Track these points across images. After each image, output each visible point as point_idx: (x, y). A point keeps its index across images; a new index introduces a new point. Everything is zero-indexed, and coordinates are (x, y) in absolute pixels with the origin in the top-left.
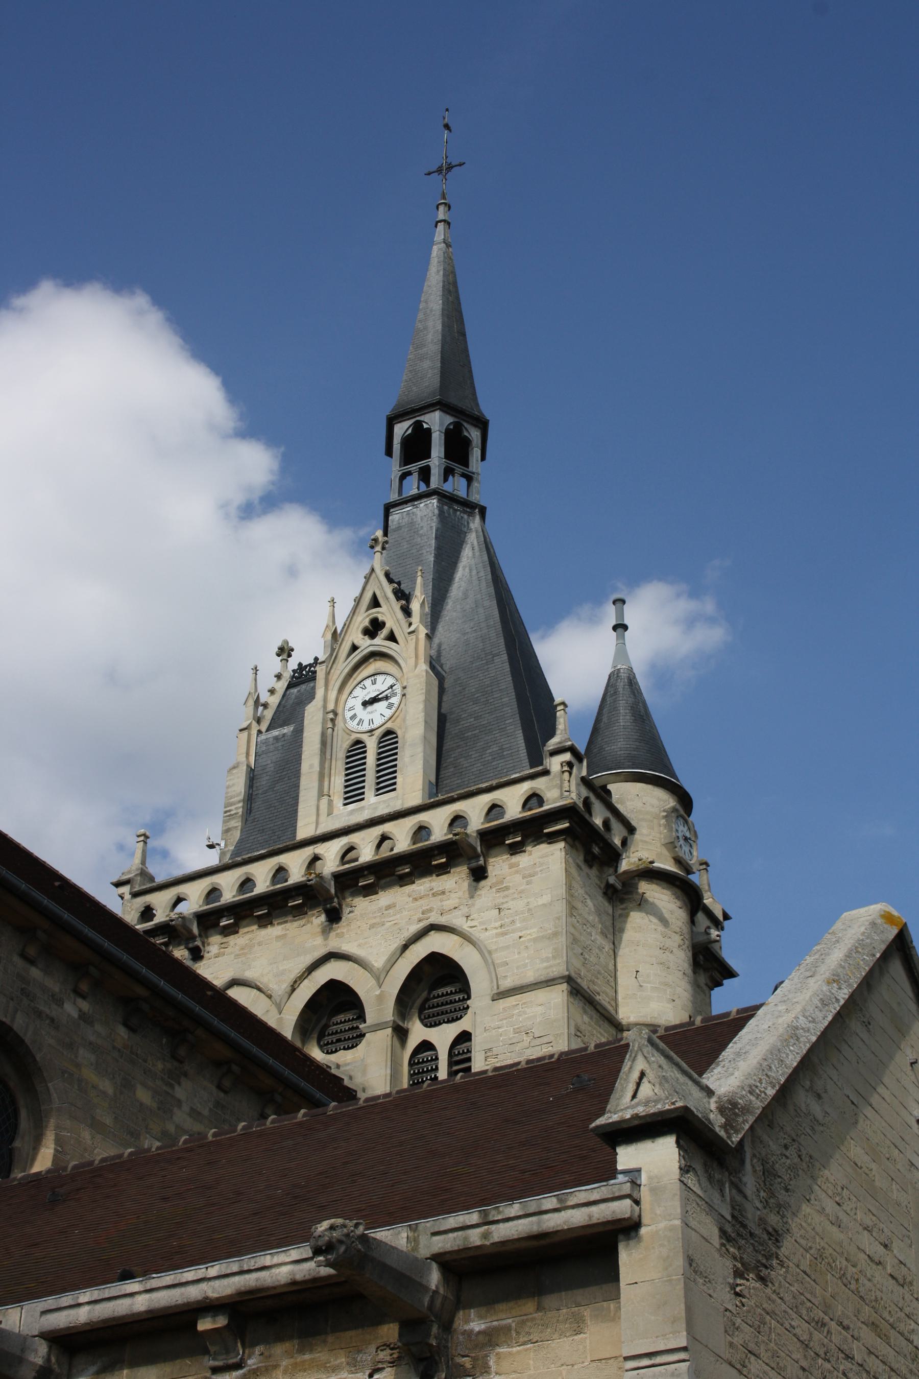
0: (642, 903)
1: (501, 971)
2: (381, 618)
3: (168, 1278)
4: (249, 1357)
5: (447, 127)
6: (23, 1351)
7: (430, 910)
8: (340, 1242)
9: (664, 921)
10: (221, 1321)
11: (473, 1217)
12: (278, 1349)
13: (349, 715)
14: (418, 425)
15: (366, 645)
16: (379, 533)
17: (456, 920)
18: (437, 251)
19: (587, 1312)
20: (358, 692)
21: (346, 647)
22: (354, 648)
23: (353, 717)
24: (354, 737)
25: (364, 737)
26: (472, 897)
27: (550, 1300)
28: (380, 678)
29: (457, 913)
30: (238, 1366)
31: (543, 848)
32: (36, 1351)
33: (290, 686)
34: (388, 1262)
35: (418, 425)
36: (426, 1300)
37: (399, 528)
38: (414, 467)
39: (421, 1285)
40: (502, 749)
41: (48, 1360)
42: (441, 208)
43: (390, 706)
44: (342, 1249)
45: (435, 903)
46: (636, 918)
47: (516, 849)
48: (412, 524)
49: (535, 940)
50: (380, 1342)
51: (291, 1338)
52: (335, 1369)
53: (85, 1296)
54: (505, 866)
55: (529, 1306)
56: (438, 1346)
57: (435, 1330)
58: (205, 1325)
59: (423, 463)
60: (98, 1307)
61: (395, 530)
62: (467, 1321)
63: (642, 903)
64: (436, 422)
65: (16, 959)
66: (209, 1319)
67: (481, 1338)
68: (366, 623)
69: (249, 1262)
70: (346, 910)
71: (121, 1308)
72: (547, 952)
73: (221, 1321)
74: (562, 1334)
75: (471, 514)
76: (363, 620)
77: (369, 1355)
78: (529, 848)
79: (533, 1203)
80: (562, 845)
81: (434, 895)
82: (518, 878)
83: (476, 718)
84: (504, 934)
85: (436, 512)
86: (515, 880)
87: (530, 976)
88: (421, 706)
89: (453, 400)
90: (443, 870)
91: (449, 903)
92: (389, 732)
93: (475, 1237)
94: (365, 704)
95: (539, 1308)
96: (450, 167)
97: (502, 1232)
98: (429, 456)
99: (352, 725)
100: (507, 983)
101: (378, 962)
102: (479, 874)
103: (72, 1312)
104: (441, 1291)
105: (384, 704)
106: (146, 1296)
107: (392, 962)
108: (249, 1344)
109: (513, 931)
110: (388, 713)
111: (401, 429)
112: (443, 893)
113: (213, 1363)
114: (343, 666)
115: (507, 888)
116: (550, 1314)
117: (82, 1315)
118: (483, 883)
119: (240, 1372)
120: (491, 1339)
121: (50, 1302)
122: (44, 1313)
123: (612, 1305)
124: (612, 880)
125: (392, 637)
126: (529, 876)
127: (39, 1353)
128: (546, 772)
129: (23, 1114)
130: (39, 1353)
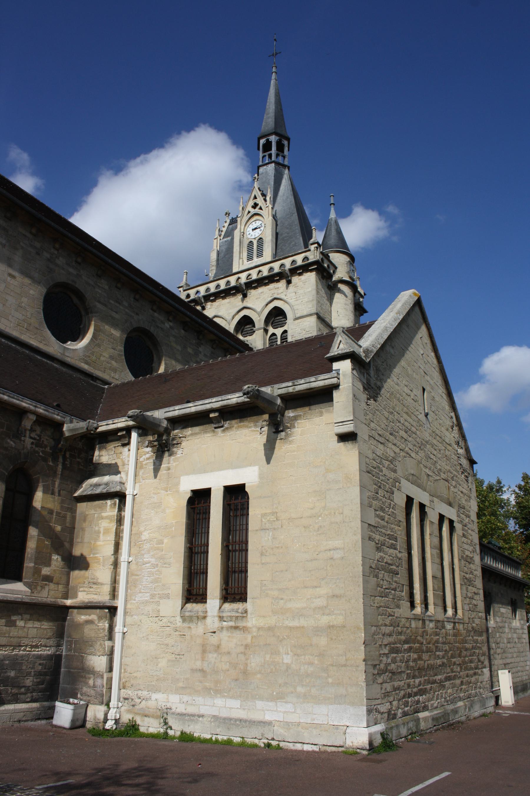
0: (339, 291)
1: (296, 312)
2: (257, 202)
3: (201, 402)
4: (225, 424)
5: (275, 40)
6: (160, 423)
7: (274, 293)
8: (251, 391)
9: (346, 296)
10: (217, 414)
11: (290, 384)
12: (234, 422)
14: (268, 140)
15: (253, 211)
16: (256, 175)
17: (282, 296)
18: (273, 82)
19: (324, 410)
20: (251, 226)
21: (247, 212)
22: (249, 212)
23: (249, 234)
24: (250, 240)
25: (253, 240)
26: (287, 289)
27: (313, 407)
28: (257, 222)
29: (282, 294)
30: (222, 427)
31: (309, 274)
32: (164, 423)
33: (229, 225)
34: (265, 397)
35: (268, 140)
36: (277, 408)
37: (262, 173)
38: (267, 154)
39: (275, 403)
40: (296, 243)
41: (167, 425)
42: (274, 68)
43: (261, 230)
44: (252, 393)
45: (276, 291)
46: (337, 296)
47: (300, 274)
48: (266, 172)
49: (307, 302)
50: (263, 420)
51: (237, 419)
52: (250, 427)
53: (177, 407)
54: (297, 279)
55: (307, 409)
56: (280, 420)
57: (279, 416)
58: (212, 415)
59: (269, 152)
60: (181, 411)
61: (261, 174)
62: (289, 413)
63: (339, 291)
64: (273, 139)
65: (150, 311)
66: (213, 414)
67: (293, 418)
68: (253, 204)
69: (224, 397)
70: (248, 294)
71: (187, 411)
72: (310, 306)
73: (217, 414)
74: (316, 417)
75: (285, 169)
76: (251, 203)
77: (260, 423)
78: (304, 274)
79: (308, 379)
80: (315, 273)
82: (301, 283)
83: (287, 234)
84: (297, 300)
85: (274, 168)
86: (300, 284)
87: (305, 313)
88: (270, 230)
89: (279, 131)
90: (278, 281)
91: (280, 291)
92: (261, 238)
93: (291, 390)
94: (253, 230)
95: (310, 409)
96: (276, 54)
97: (298, 388)
98: (271, 150)
99: (249, 236)
100: (298, 315)
101: (259, 310)
102: (289, 282)
103: (173, 412)
104: (281, 405)
105: (259, 230)
106: (195, 407)
107: (263, 309)
108: (225, 420)
109: (300, 299)
110: (260, 232)
111: (262, 141)
112: (278, 288)
113: (215, 426)
114: (246, 218)
115: (298, 286)
116: (313, 411)
117: (176, 413)
118: (290, 285)
119: (223, 428)
120: (296, 418)
121: (167, 409)
122: (165, 412)
123: (331, 408)
124: (330, 283)
125: (261, 209)
126: (304, 283)
127: (165, 424)
128: (309, 250)
129: (155, 356)
130: (165, 424)
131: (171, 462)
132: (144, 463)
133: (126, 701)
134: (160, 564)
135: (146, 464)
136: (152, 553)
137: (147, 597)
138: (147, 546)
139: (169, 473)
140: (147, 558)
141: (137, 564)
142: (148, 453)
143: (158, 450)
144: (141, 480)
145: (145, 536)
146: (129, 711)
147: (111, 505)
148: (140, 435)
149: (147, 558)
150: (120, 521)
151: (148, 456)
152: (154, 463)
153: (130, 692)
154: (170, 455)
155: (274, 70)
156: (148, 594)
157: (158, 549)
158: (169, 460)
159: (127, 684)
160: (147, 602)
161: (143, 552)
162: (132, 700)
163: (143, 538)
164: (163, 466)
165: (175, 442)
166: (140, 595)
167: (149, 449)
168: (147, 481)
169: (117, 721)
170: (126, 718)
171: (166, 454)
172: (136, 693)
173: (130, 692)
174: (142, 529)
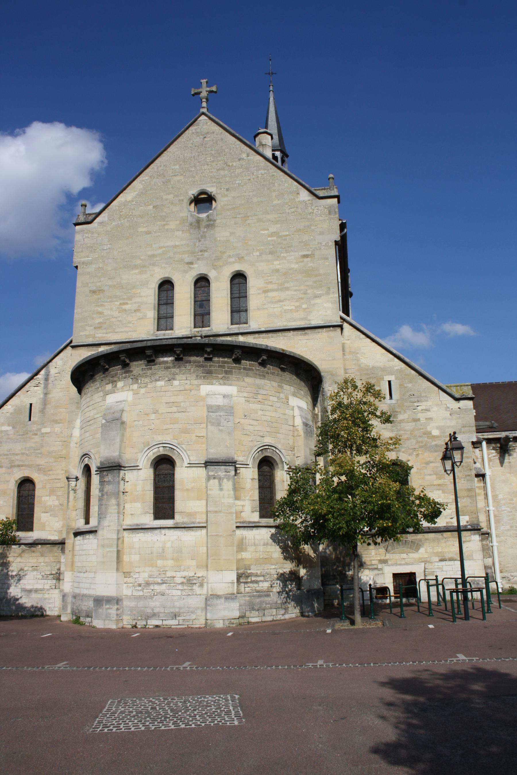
5: (270, 60)
18: (272, 99)
42: (271, 86)
89: (282, 149)
96: (272, 74)
121: (510, 432)
131: (511, 459)
132: (492, 458)
133: (504, 579)
134: (513, 511)
135: (493, 459)
136: (507, 506)
137: (508, 527)
138: (503, 502)
139: (510, 465)
140: (504, 508)
141: (498, 511)
142: (493, 453)
143: (500, 452)
144: (492, 468)
145: (501, 496)
146: (507, 583)
147: (478, 481)
148: (487, 443)
149: (504, 508)
150: (485, 488)
151: (494, 455)
152: (499, 459)
153: (506, 574)
154: (510, 455)
155: (271, 88)
156: (508, 526)
157: (511, 503)
158: (509, 458)
159: (503, 571)
160: (508, 530)
161: (500, 505)
162: (508, 577)
163: (499, 498)
164: (506, 460)
165: (511, 449)
166: (503, 526)
167: (494, 451)
168: (496, 468)
169: (502, 588)
170: (507, 586)
171: (507, 455)
172: (510, 574)
173: (506, 574)
174: (497, 493)
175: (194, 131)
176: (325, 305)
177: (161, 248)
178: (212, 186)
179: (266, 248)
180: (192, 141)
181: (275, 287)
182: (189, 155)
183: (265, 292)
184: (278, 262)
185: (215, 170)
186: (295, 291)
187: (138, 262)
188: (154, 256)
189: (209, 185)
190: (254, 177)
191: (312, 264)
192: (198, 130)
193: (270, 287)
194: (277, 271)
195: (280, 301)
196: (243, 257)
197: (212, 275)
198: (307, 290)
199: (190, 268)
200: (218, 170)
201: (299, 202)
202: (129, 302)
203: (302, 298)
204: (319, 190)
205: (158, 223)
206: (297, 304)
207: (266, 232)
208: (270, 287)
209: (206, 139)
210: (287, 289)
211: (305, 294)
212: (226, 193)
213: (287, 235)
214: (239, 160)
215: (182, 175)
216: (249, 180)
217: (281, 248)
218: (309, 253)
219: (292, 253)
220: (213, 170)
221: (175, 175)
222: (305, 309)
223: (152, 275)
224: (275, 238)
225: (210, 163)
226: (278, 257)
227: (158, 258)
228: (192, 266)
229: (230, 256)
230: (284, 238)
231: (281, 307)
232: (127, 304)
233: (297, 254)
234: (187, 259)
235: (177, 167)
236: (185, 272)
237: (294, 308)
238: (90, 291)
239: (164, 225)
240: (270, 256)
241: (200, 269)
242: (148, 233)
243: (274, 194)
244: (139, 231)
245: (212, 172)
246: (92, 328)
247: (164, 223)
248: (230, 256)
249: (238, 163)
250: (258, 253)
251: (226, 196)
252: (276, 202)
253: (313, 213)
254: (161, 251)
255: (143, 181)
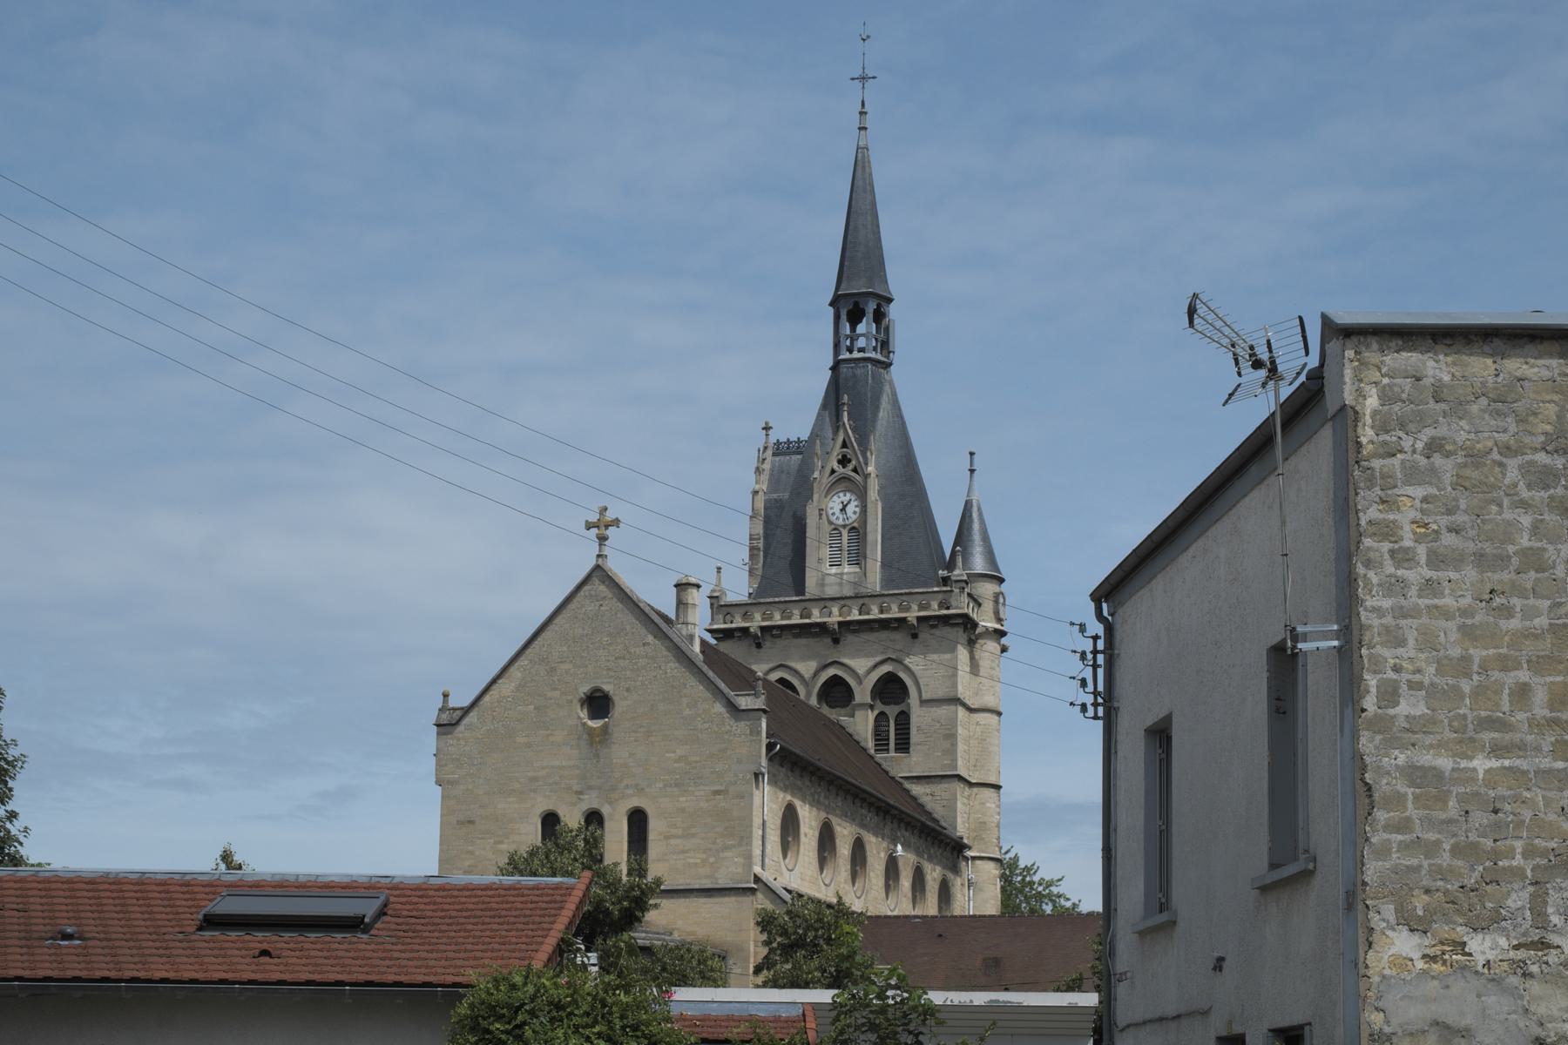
13: (830, 512)
21: (828, 470)
22: (833, 471)
47: (933, 627)
49: (943, 676)
70: (842, 639)
81: (891, 640)
101: (861, 672)
107: (869, 672)
109: (932, 669)
175: (587, 593)
176: (736, 859)
177: (543, 768)
178: (610, 683)
179: (672, 779)
180: (584, 610)
181: (680, 832)
182: (580, 631)
183: (667, 838)
184: (684, 799)
185: (613, 658)
186: (703, 839)
187: (517, 786)
188: (534, 779)
189: (605, 680)
190: (661, 672)
191: (724, 804)
192: (593, 593)
193: (674, 831)
194: (683, 810)
195: (683, 852)
196: (643, 789)
197: (606, 810)
198: (716, 838)
199: (580, 799)
200: (616, 659)
201: (715, 714)
202: (506, 841)
203: (710, 849)
204: (741, 695)
205: (541, 732)
206: (704, 856)
207: (673, 755)
208: (674, 831)
209: (602, 608)
210: (693, 835)
211: (714, 843)
212: (626, 694)
213: (697, 762)
214: (644, 644)
215: (571, 662)
216: (656, 676)
217: (690, 779)
218: (723, 788)
219: (702, 787)
220: (610, 658)
221: (561, 662)
222: (712, 864)
223: (533, 806)
224: (683, 764)
225: (606, 647)
226: (685, 791)
227: (541, 783)
228: (582, 797)
229: (627, 787)
230: (694, 765)
231: (684, 859)
232: (502, 843)
233: (707, 788)
234: (576, 788)
235: (565, 649)
236: (574, 804)
237: (699, 861)
238: (458, 821)
239: (548, 735)
240: (675, 789)
241: (591, 801)
242: (529, 745)
243: (685, 701)
244: (518, 741)
245: (609, 661)
246: (461, 872)
247: (549, 732)
248: (627, 787)
249: (642, 649)
250: (661, 785)
251: (626, 699)
252: (687, 712)
253: (731, 731)
254: (543, 773)
255: (522, 666)
